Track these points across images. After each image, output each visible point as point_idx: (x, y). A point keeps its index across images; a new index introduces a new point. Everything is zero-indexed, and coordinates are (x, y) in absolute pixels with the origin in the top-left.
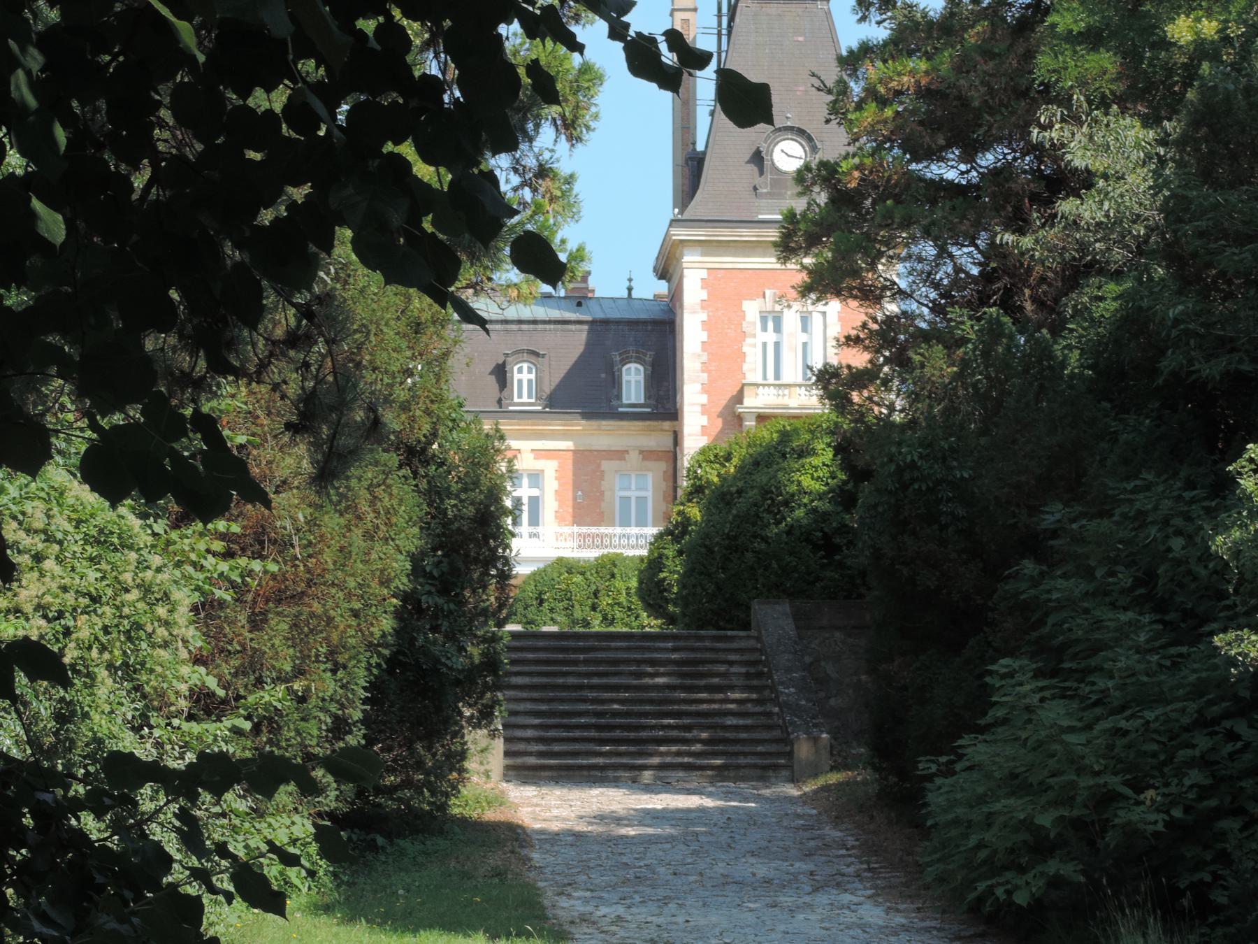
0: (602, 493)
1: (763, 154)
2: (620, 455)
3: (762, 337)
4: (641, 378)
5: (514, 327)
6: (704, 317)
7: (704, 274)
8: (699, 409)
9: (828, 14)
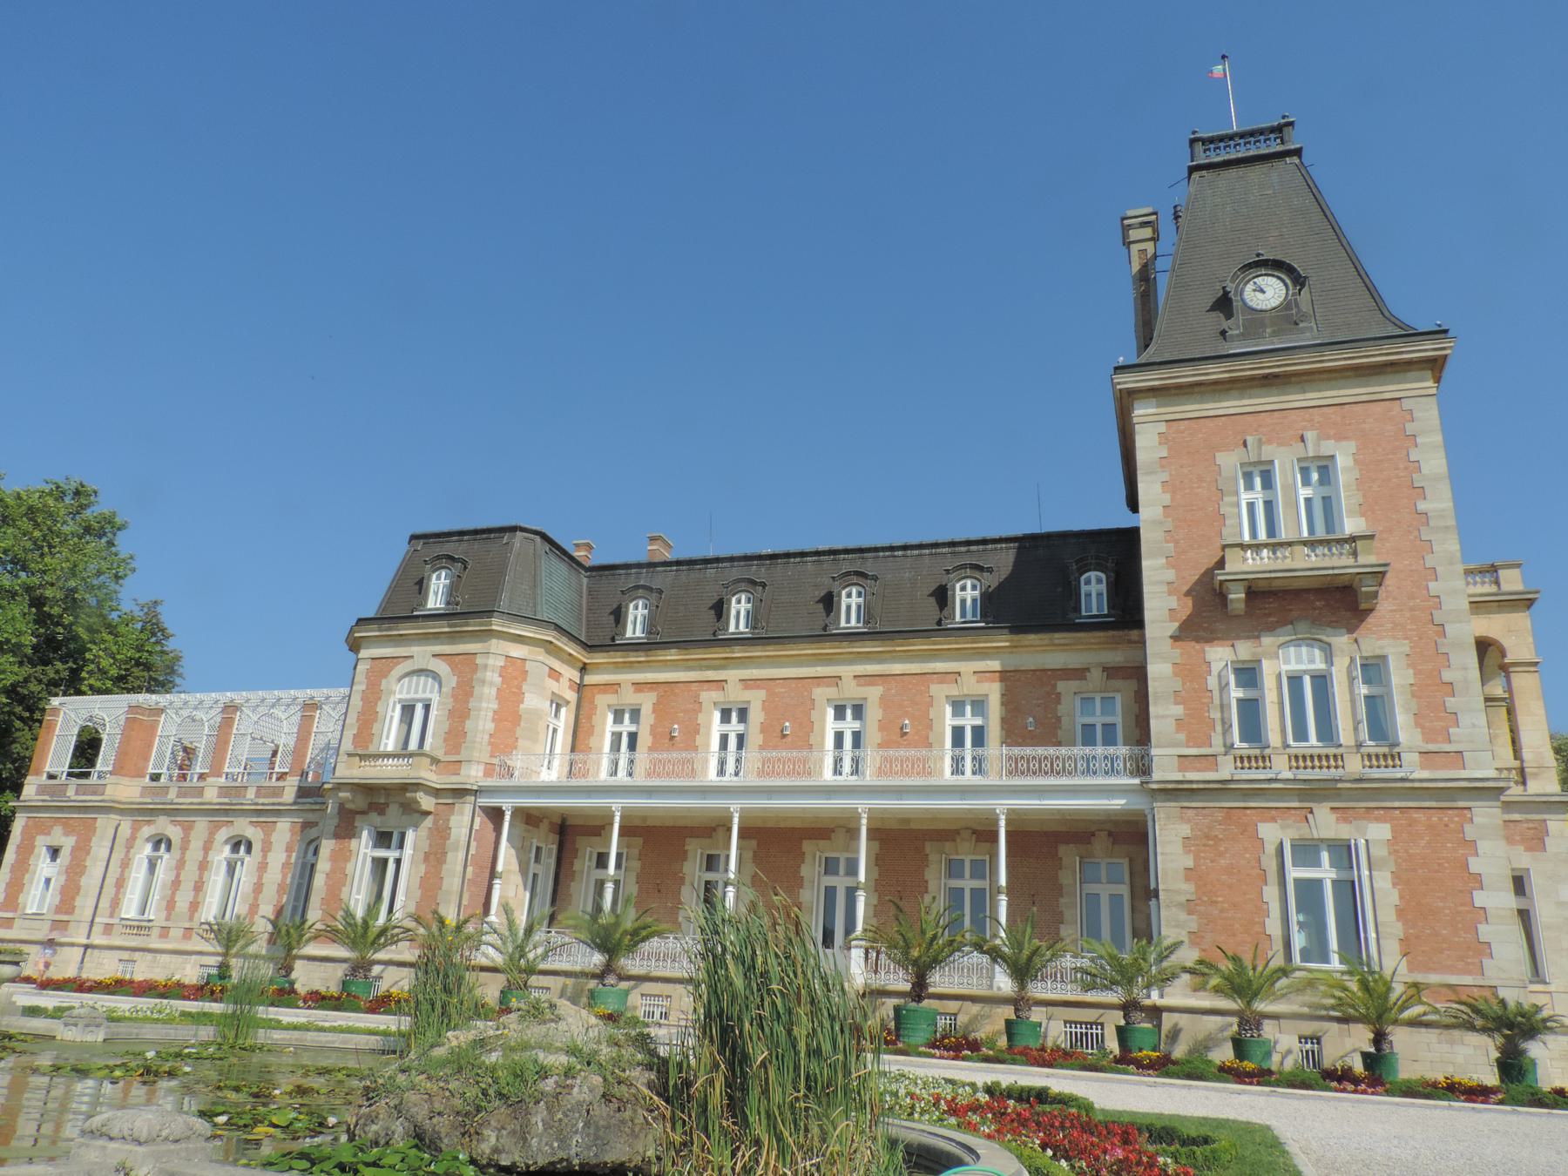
0: (1059, 719)
1: (1231, 295)
2: (1079, 674)
3: (1245, 497)
4: (1103, 587)
5: (963, 549)
6: (1165, 477)
7: (1162, 428)
8: (1165, 588)
9: (1301, 167)
